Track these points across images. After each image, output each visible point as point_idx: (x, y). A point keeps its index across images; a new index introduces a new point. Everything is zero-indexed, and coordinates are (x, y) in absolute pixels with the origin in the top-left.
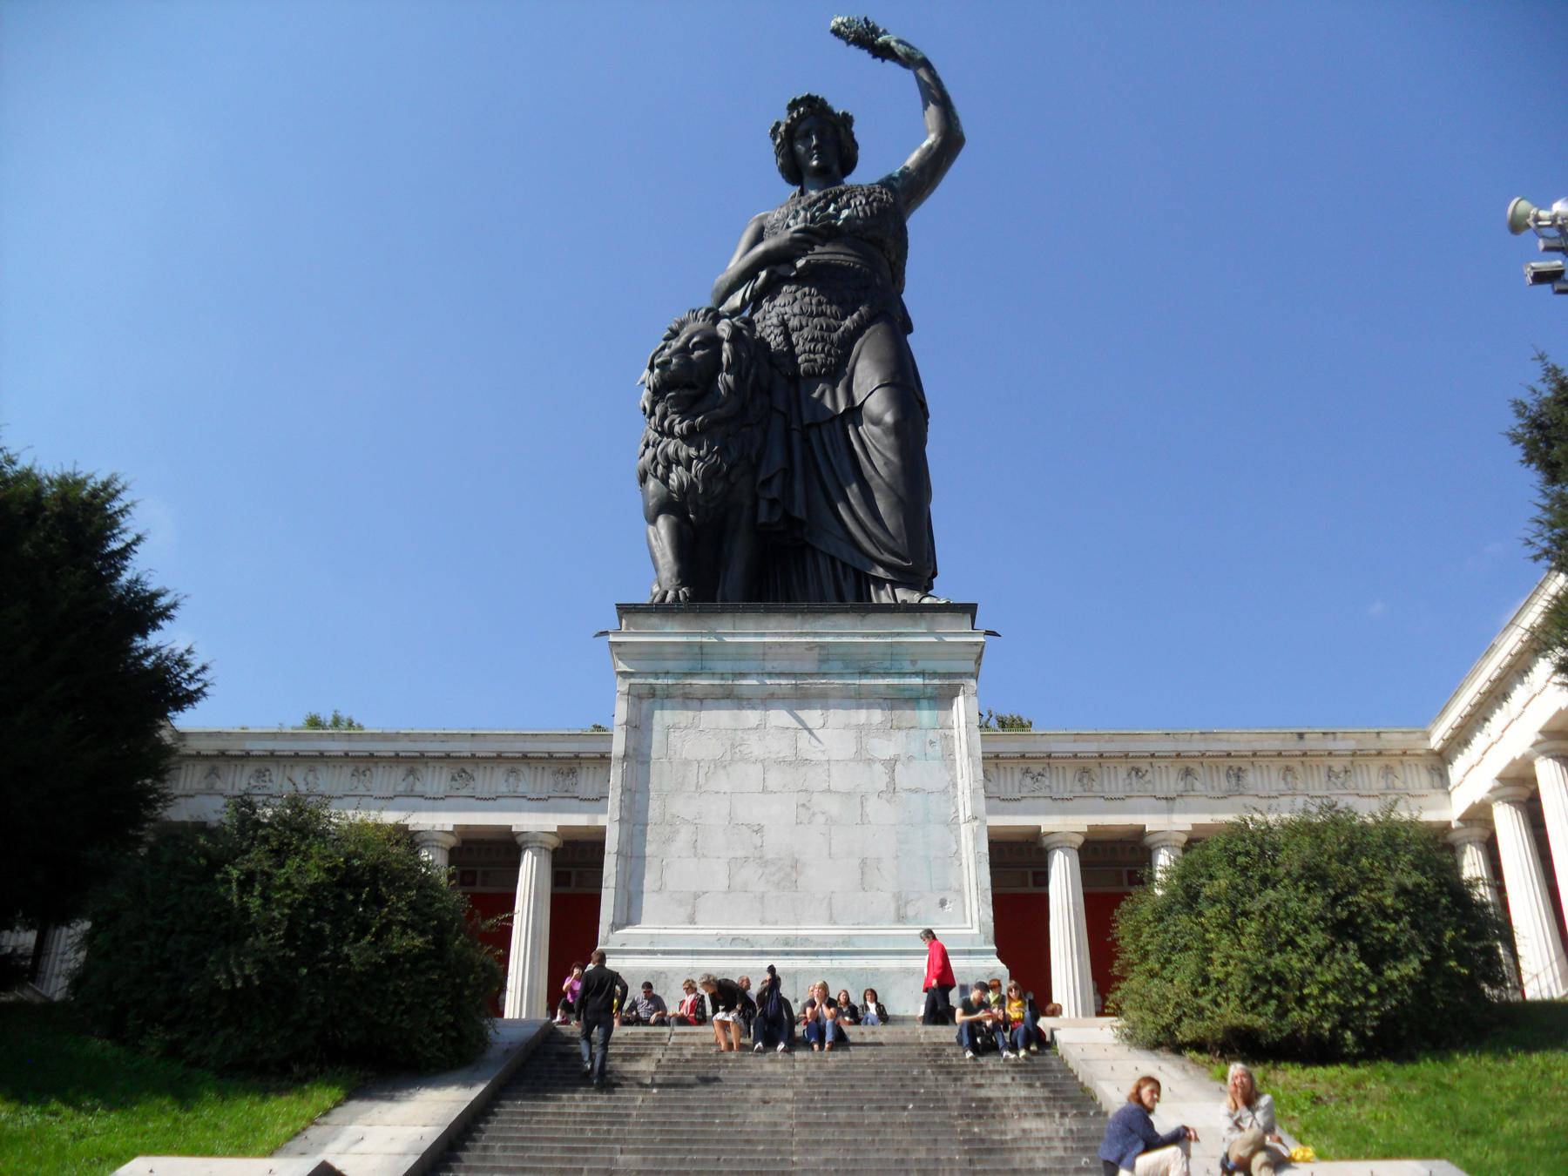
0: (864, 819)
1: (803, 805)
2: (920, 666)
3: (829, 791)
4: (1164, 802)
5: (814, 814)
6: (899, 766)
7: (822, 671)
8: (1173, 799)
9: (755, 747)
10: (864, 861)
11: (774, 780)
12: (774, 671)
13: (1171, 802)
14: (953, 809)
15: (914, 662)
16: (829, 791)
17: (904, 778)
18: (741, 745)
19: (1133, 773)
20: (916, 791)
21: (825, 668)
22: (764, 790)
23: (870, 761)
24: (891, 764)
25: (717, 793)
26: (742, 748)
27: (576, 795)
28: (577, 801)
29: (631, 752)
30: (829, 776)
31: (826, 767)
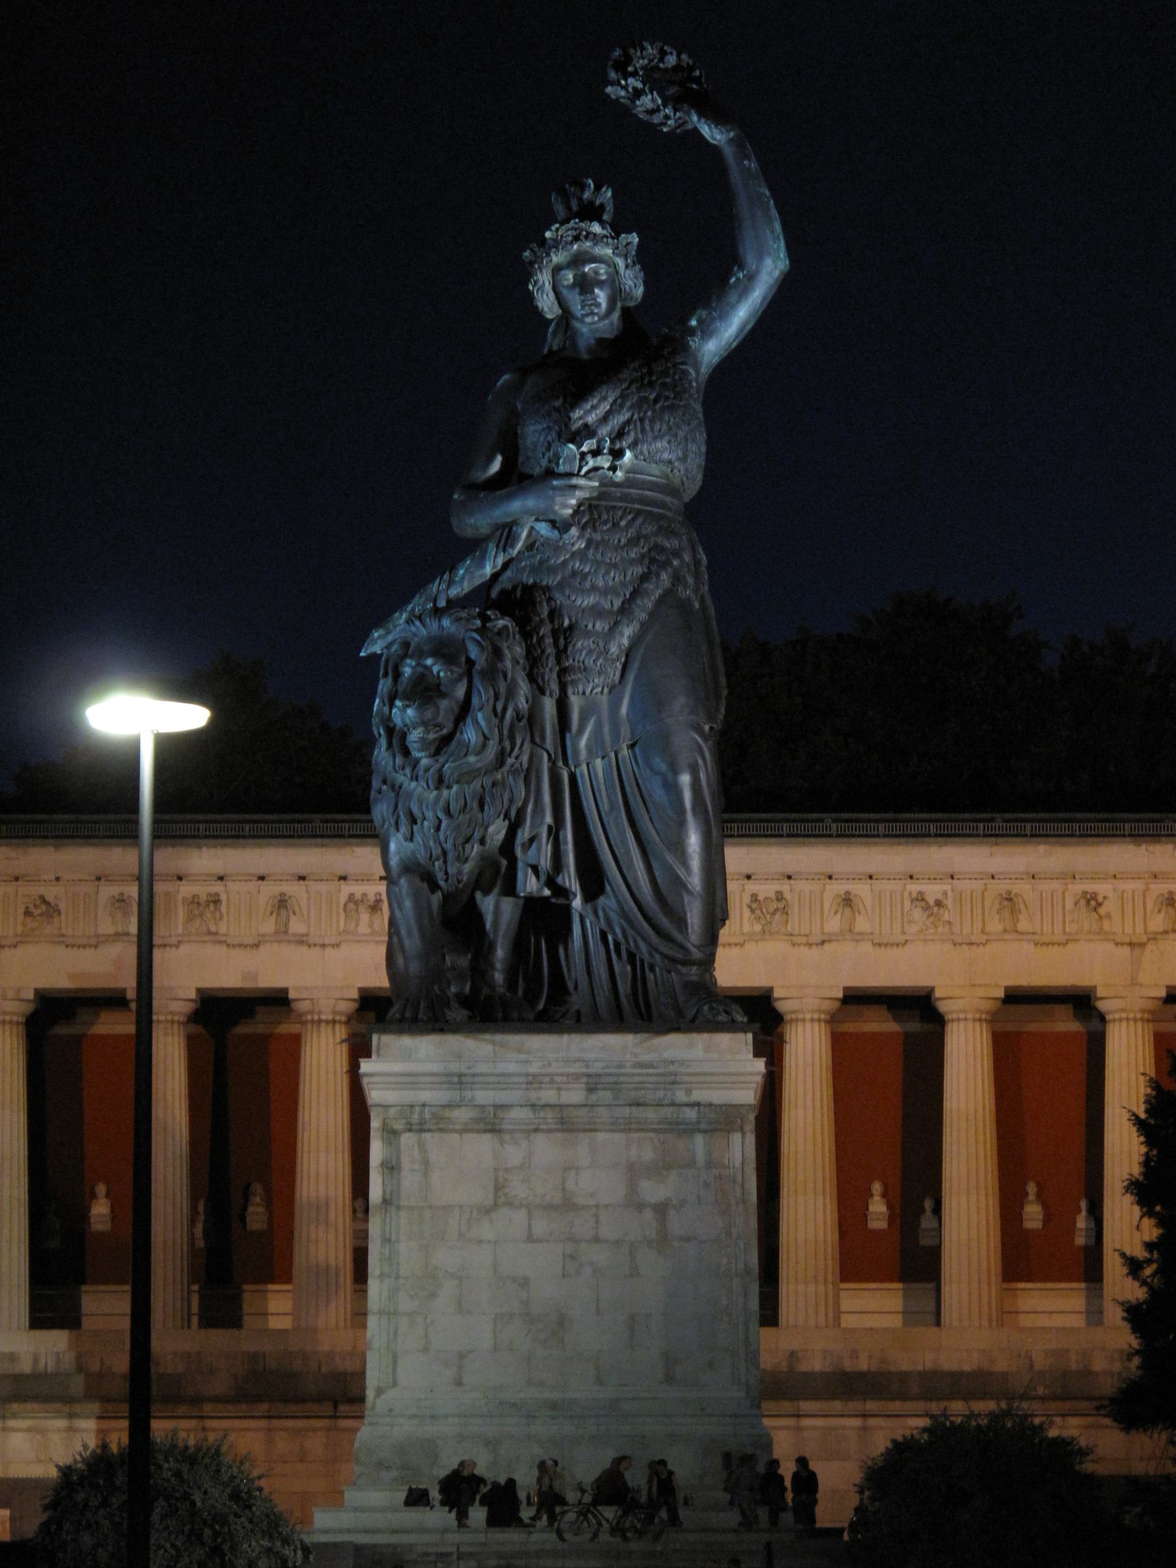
0: (634, 1272)
1: (571, 1257)
2: (698, 1095)
3: (597, 1240)
4: (1126, 950)
5: (581, 1265)
6: (672, 1212)
7: (590, 1102)
8: (1142, 945)
9: (518, 1189)
10: (633, 1317)
11: (541, 1226)
12: (537, 1102)
13: (1137, 951)
14: (725, 1261)
15: (689, 1092)
16: (597, 1240)
17: (676, 1224)
18: (503, 1187)
19: (1083, 902)
20: (688, 1239)
21: (594, 1097)
22: (530, 1238)
23: (640, 1207)
24: (661, 1209)
25: (480, 1241)
26: (507, 1190)
27: (223, 938)
28: (224, 948)
29: (388, 1197)
30: (597, 1222)
31: (594, 1210)
